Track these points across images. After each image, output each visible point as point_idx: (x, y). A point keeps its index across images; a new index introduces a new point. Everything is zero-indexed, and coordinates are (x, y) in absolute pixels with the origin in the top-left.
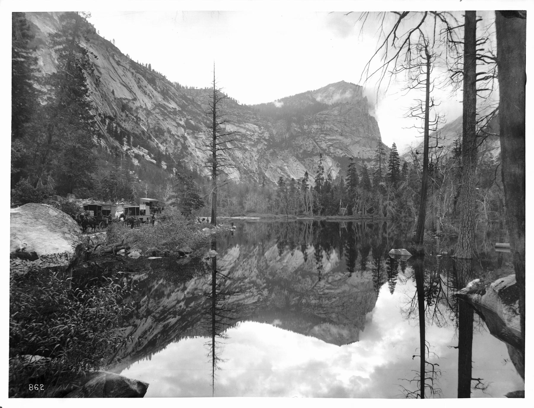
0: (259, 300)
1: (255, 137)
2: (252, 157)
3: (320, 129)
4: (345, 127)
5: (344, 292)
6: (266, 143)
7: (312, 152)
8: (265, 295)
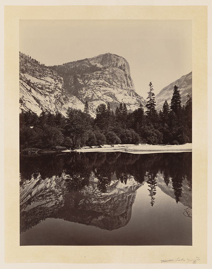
0: (56, 204)
1: (52, 87)
2: (51, 100)
3: (96, 83)
4: (113, 82)
5: (115, 194)
6: (60, 91)
7: (92, 98)
8: (61, 200)
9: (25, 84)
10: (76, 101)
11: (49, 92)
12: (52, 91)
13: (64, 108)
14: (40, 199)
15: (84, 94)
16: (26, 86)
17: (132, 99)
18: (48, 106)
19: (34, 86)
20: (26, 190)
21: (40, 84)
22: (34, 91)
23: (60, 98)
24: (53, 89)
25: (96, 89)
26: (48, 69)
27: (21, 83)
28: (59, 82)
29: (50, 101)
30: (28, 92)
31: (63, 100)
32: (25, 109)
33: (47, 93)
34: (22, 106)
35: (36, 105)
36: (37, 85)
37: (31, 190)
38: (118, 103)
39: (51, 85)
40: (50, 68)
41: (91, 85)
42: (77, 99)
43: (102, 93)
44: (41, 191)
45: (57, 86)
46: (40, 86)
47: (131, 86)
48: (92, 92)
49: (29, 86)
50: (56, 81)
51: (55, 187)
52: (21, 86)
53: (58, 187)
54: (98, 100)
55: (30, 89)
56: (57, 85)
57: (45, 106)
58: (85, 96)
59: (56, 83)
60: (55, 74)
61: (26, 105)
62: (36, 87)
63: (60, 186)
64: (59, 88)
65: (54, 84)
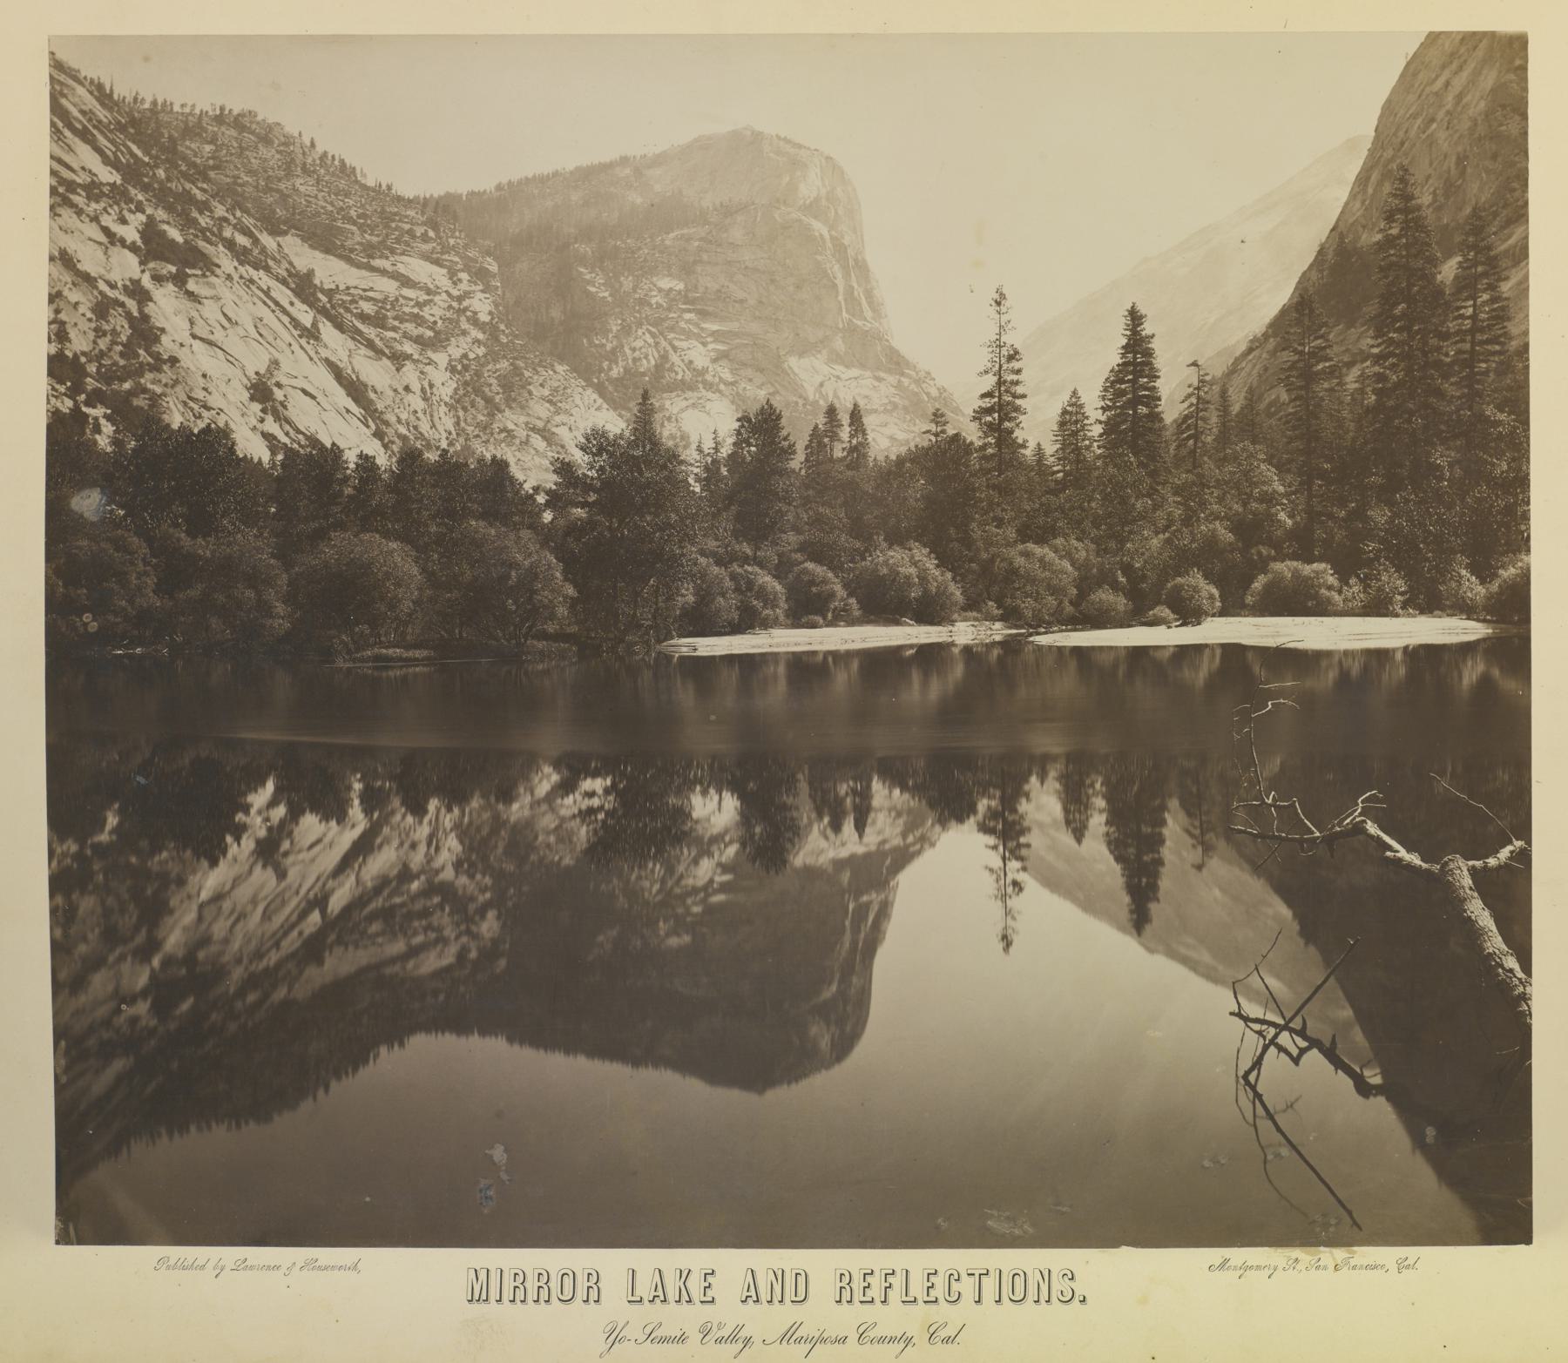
0: (462, 956)
2: (431, 386)
6: (481, 336)
9: (283, 294)
10: (569, 391)
11: (418, 340)
12: (437, 333)
13: (501, 431)
14: (377, 935)
15: (612, 356)
16: (292, 304)
17: (876, 384)
18: (412, 418)
19: (333, 307)
20: (296, 885)
21: (371, 294)
22: (336, 332)
23: (478, 374)
24: (440, 323)
25: (682, 324)
26: (411, 213)
27: (262, 290)
28: (474, 288)
29: (423, 390)
30: (303, 341)
31: (496, 388)
32: (287, 434)
33: (408, 348)
34: (269, 419)
35: (348, 411)
36: (353, 301)
37: (324, 885)
38: (797, 403)
39: (431, 301)
40: (423, 204)
41: (650, 305)
42: (576, 383)
43: (711, 346)
44: (377, 890)
45: (466, 309)
46: (368, 308)
47: (868, 314)
48: (657, 344)
49: (305, 307)
50: (460, 280)
51: (458, 865)
52: (265, 303)
53: (472, 865)
54: (692, 388)
55: (314, 324)
56: (465, 304)
57: (399, 421)
58: (617, 363)
59: (455, 293)
60: (452, 241)
61: (292, 413)
62: (348, 310)
63: (485, 859)
64: (474, 321)
65: (446, 292)
